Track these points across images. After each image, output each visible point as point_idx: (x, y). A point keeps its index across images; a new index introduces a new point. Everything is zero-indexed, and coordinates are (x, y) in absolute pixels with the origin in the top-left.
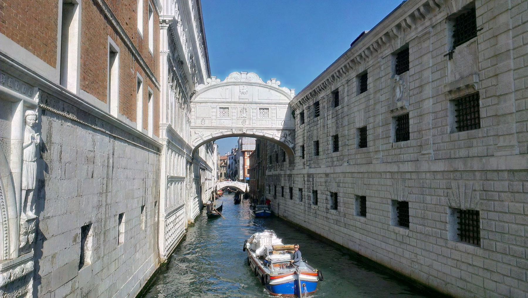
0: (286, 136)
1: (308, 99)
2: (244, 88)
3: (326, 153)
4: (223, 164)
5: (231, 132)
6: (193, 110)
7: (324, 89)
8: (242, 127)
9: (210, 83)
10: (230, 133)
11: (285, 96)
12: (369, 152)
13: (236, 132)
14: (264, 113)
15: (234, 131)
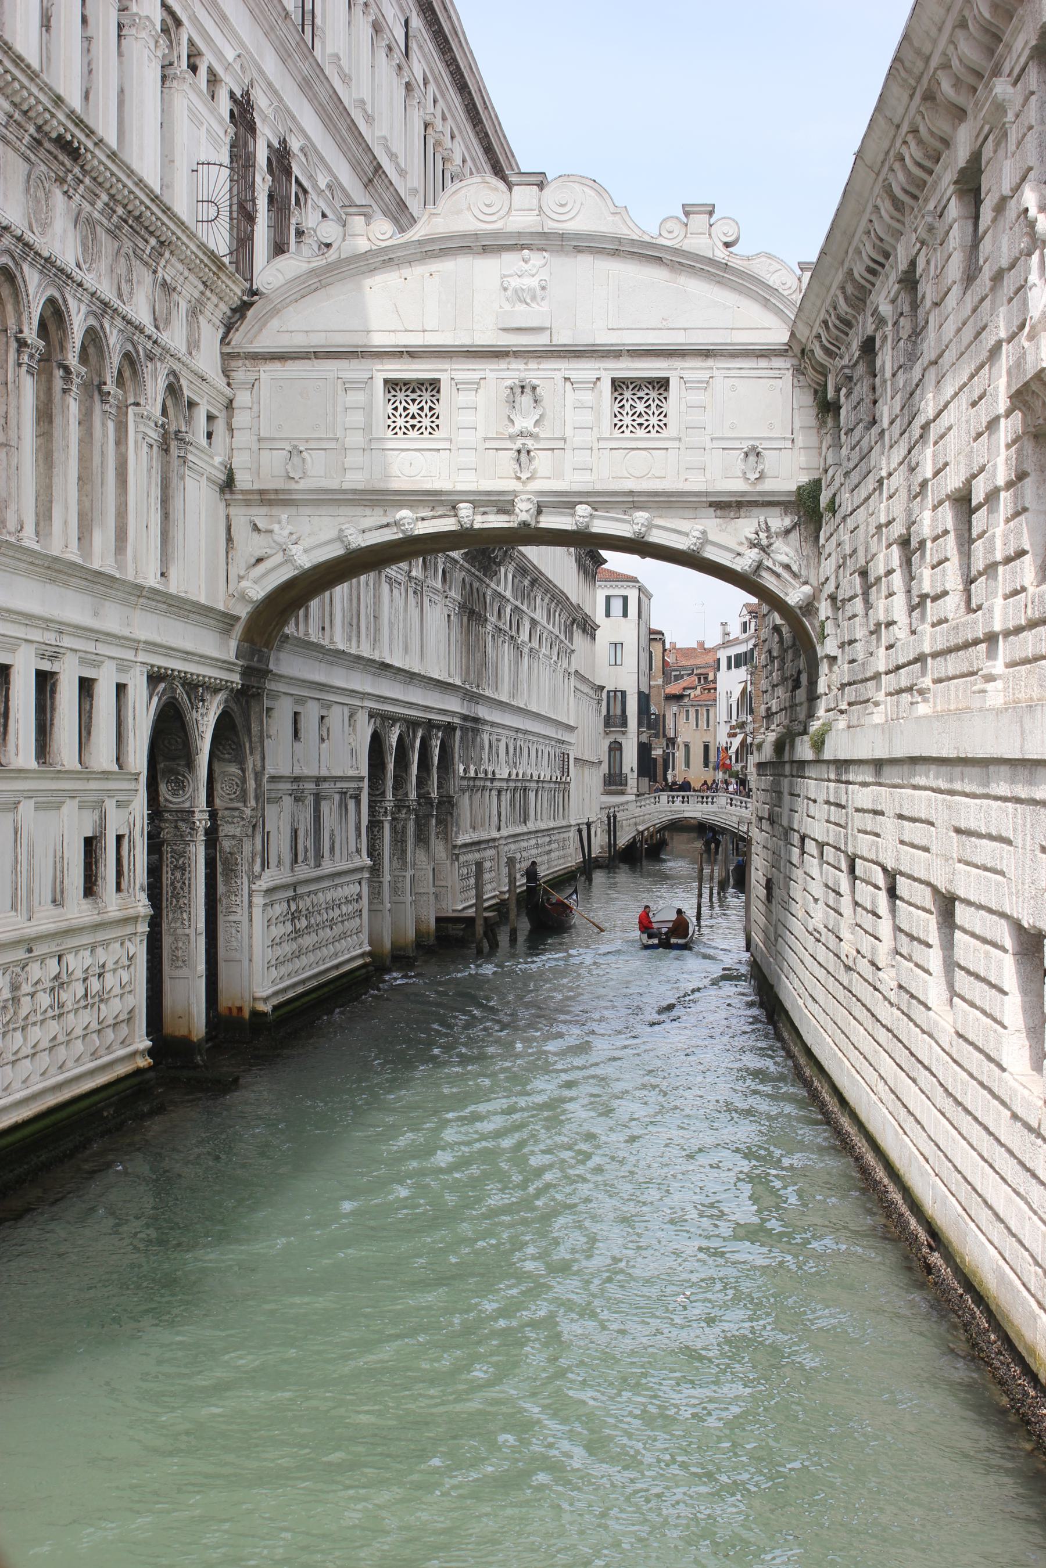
0: (764, 542)
1: (849, 324)
2: (526, 267)
3: (884, 643)
4: (698, 691)
5: (453, 520)
6: (242, 398)
7: (883, 266)
8: (515, 494)
9: (335, 246)
10: (448, 525)
11: (766, 303)
12: (976, 642)
13: (479, 518)
14: (640, 407)
15: (465, 510)
